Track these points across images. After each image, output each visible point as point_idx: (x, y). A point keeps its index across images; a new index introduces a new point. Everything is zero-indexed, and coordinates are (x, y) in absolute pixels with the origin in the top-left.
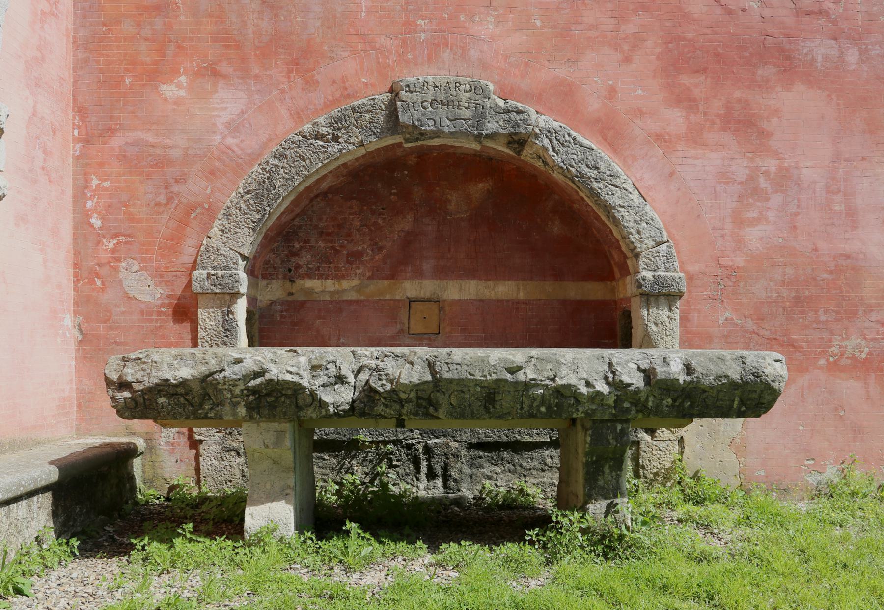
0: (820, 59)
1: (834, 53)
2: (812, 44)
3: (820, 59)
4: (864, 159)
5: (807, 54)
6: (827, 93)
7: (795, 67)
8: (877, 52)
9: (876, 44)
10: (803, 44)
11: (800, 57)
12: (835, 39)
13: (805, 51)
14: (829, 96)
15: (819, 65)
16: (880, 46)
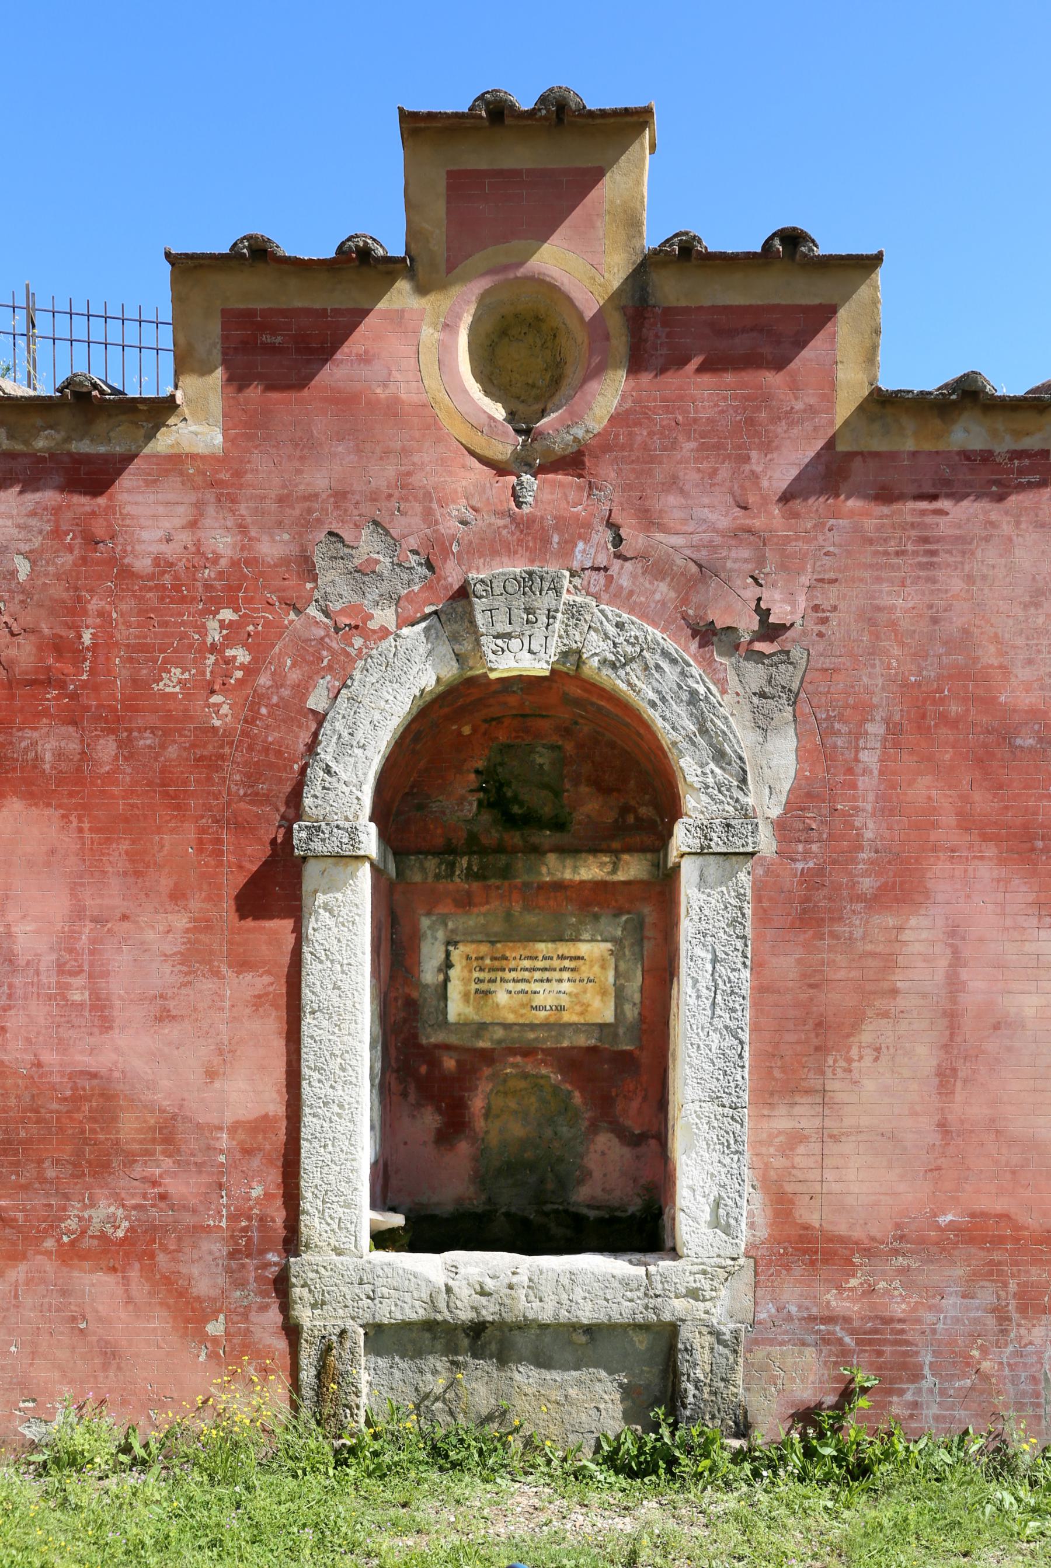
0: (48, 757)
1: (74, 746)
2: (36, 735)
3: (48, 757)
4: (125, 917)
5: (26, 750)
6: (62, 812)
7: (7, 772)
8: (148, 742)
9: (146, 729)
10: (20, 734)
11: (15, 756)
12: (74, 723)
13: (23, 744)
14: (63, 816)
15: (47, 767)
16: (152, 732)
